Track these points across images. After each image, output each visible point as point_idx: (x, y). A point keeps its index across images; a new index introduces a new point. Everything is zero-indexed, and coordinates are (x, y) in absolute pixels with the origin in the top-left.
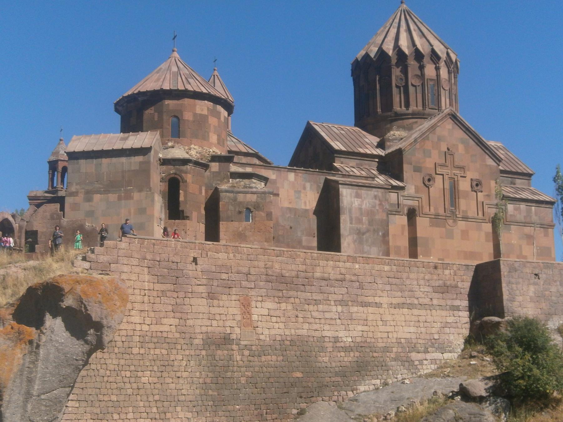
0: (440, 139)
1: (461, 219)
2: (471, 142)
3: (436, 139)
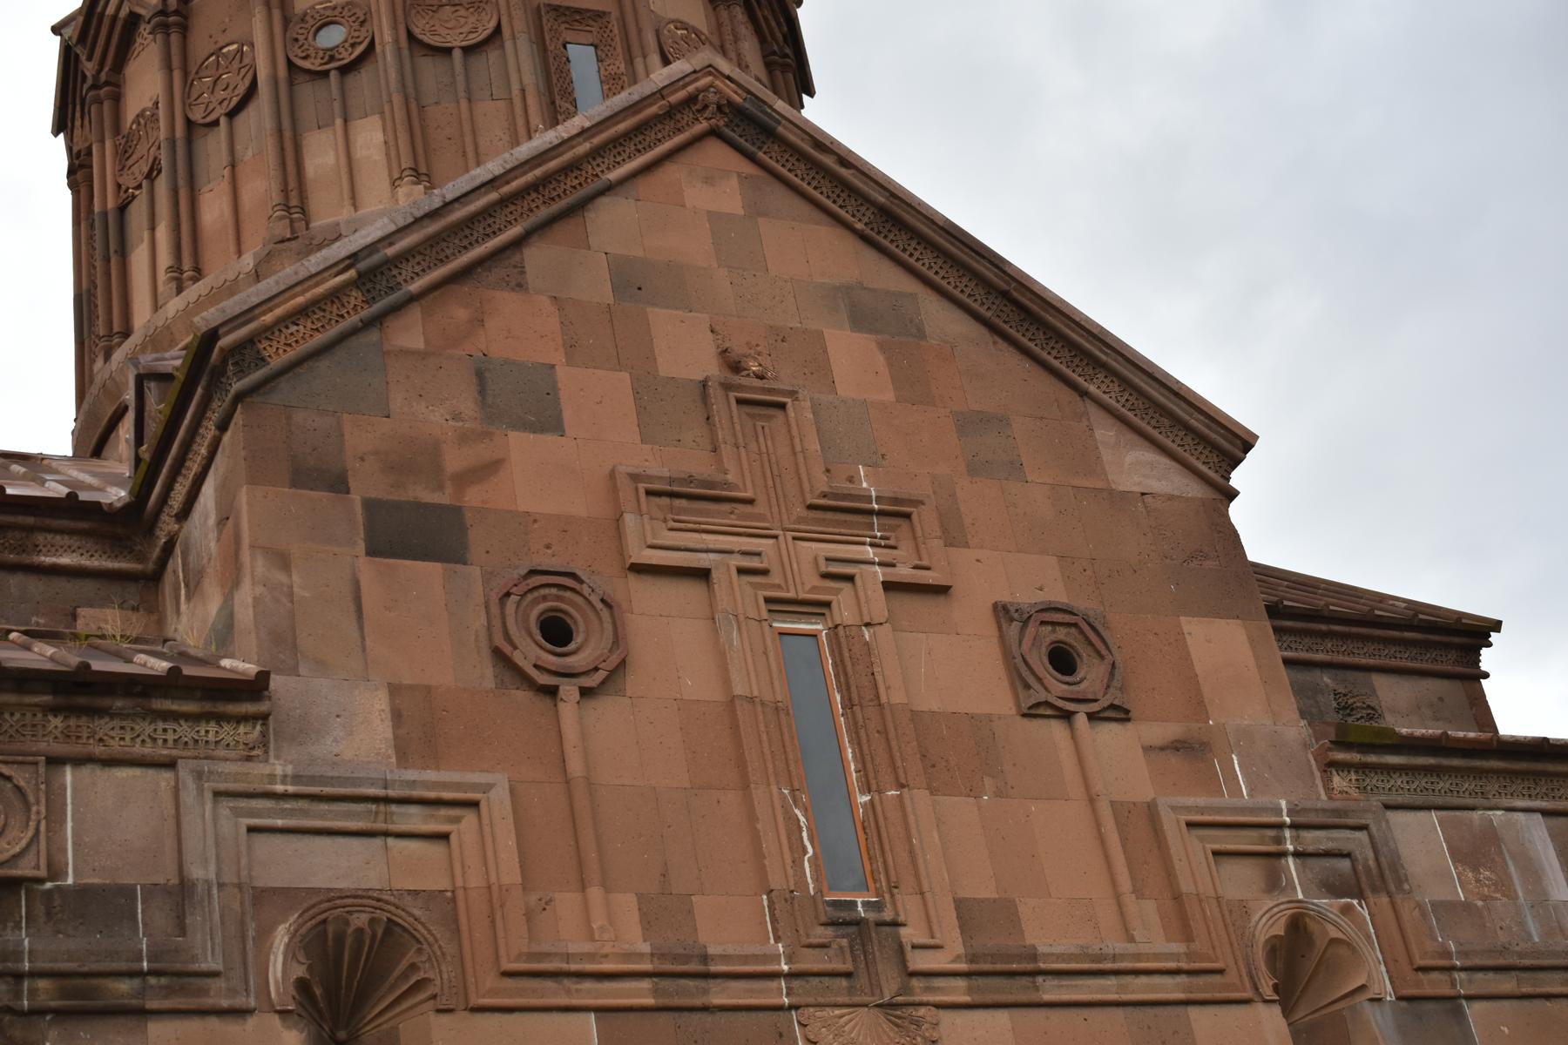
0: (634, 283)
1: (958, 991)
2: (942, 321)
3: (594, 286)
